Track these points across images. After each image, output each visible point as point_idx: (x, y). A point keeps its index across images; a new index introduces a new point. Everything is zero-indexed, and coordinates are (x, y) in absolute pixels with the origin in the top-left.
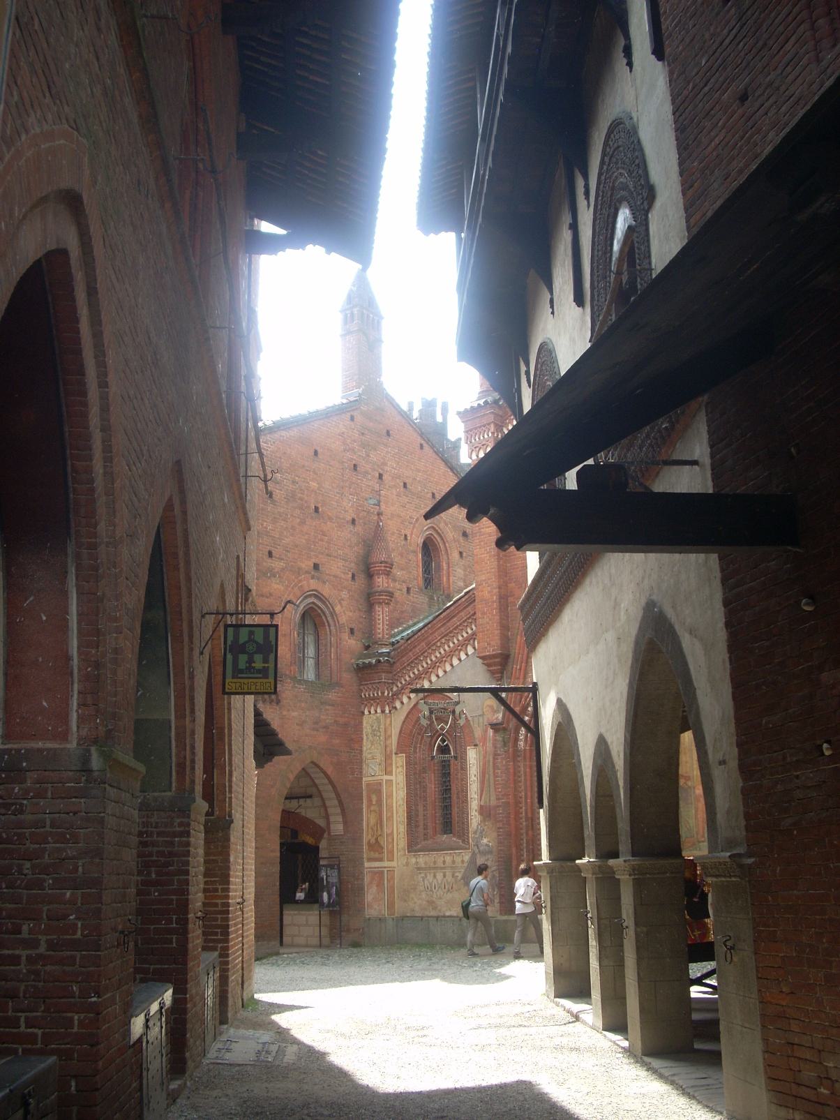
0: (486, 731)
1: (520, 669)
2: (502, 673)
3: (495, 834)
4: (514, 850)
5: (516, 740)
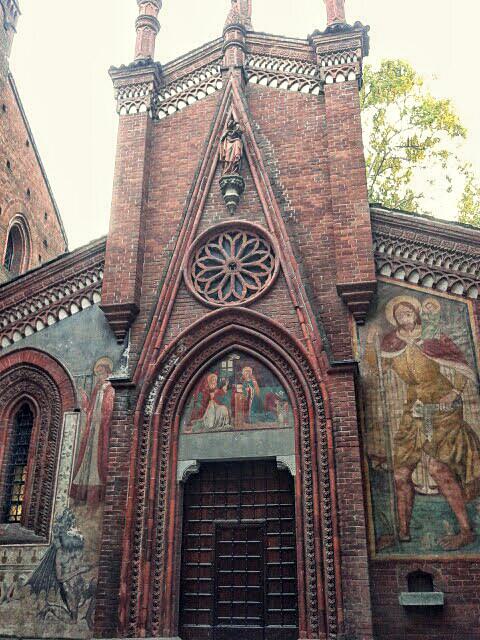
0: (93, 394)
1: (161, 321)
2: (127, 330)
3: (95, 524)
4: (126, 544)
5: (145, 402)
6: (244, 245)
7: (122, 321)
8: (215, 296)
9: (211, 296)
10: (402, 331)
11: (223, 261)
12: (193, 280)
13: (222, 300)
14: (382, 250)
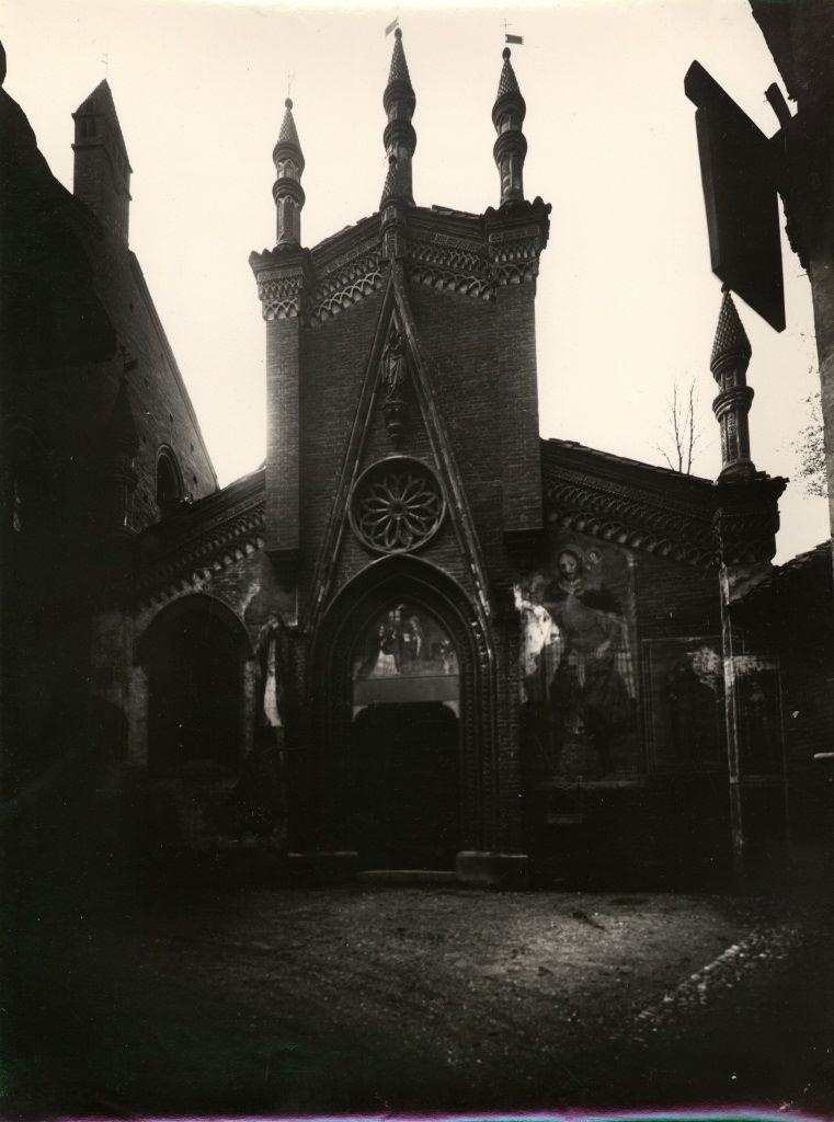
6: (410, 485)
7: (289, 569)
8: (381, 542)
9: (377, 542)
10: (566, 582)
11: (387, 503)
12: (358, 523)
13: (389, 546)
14: (549, 494)
